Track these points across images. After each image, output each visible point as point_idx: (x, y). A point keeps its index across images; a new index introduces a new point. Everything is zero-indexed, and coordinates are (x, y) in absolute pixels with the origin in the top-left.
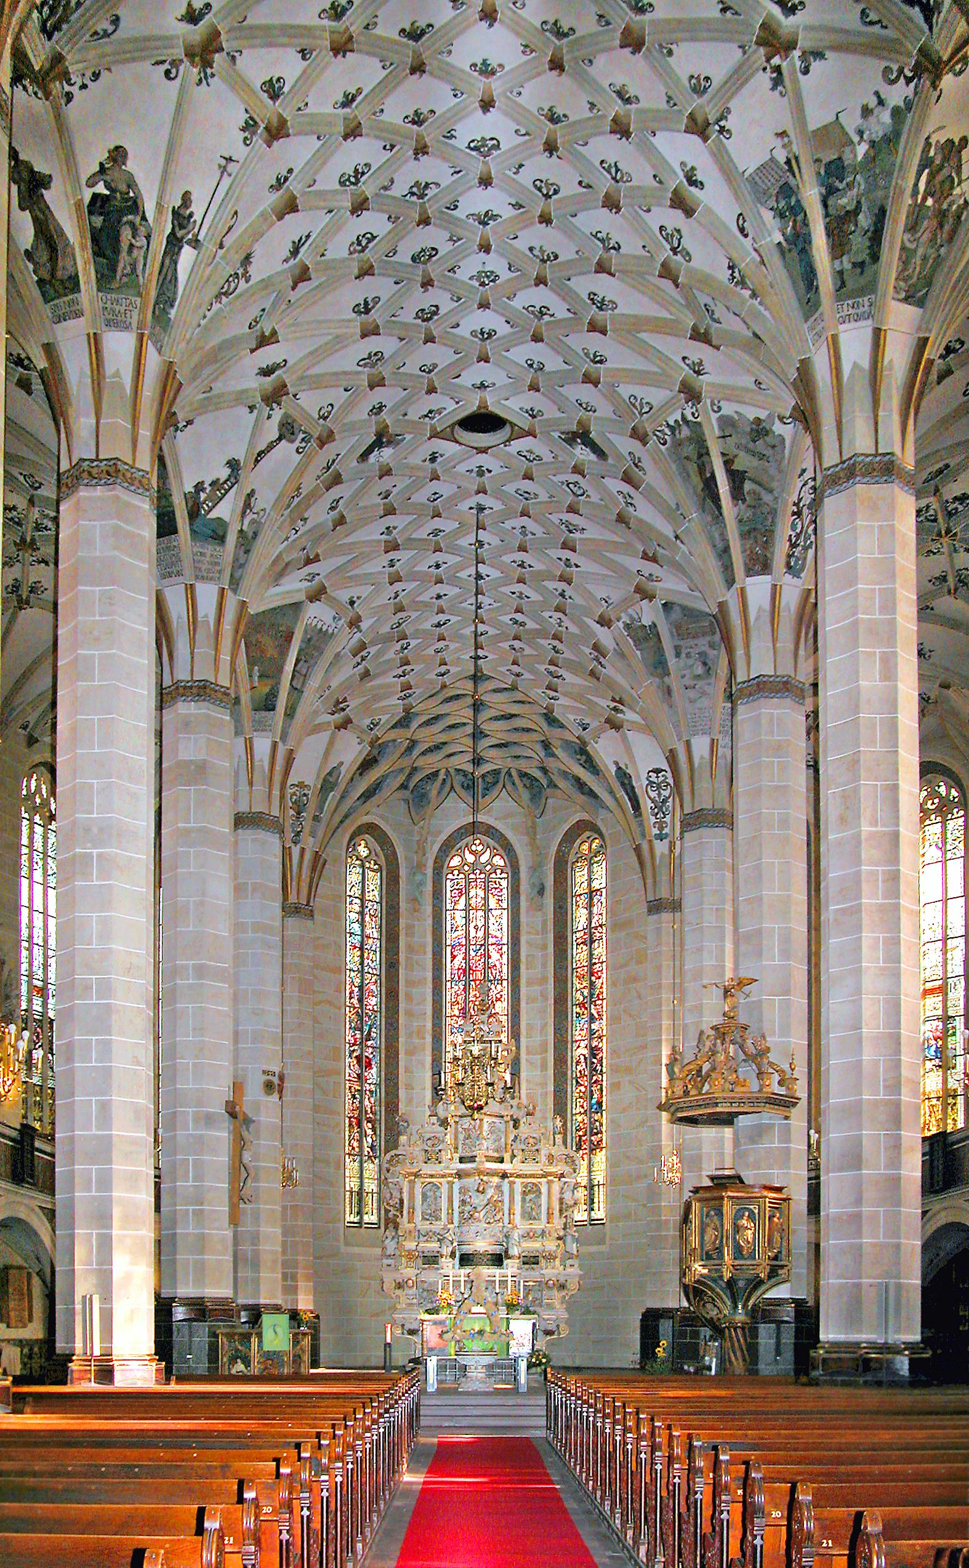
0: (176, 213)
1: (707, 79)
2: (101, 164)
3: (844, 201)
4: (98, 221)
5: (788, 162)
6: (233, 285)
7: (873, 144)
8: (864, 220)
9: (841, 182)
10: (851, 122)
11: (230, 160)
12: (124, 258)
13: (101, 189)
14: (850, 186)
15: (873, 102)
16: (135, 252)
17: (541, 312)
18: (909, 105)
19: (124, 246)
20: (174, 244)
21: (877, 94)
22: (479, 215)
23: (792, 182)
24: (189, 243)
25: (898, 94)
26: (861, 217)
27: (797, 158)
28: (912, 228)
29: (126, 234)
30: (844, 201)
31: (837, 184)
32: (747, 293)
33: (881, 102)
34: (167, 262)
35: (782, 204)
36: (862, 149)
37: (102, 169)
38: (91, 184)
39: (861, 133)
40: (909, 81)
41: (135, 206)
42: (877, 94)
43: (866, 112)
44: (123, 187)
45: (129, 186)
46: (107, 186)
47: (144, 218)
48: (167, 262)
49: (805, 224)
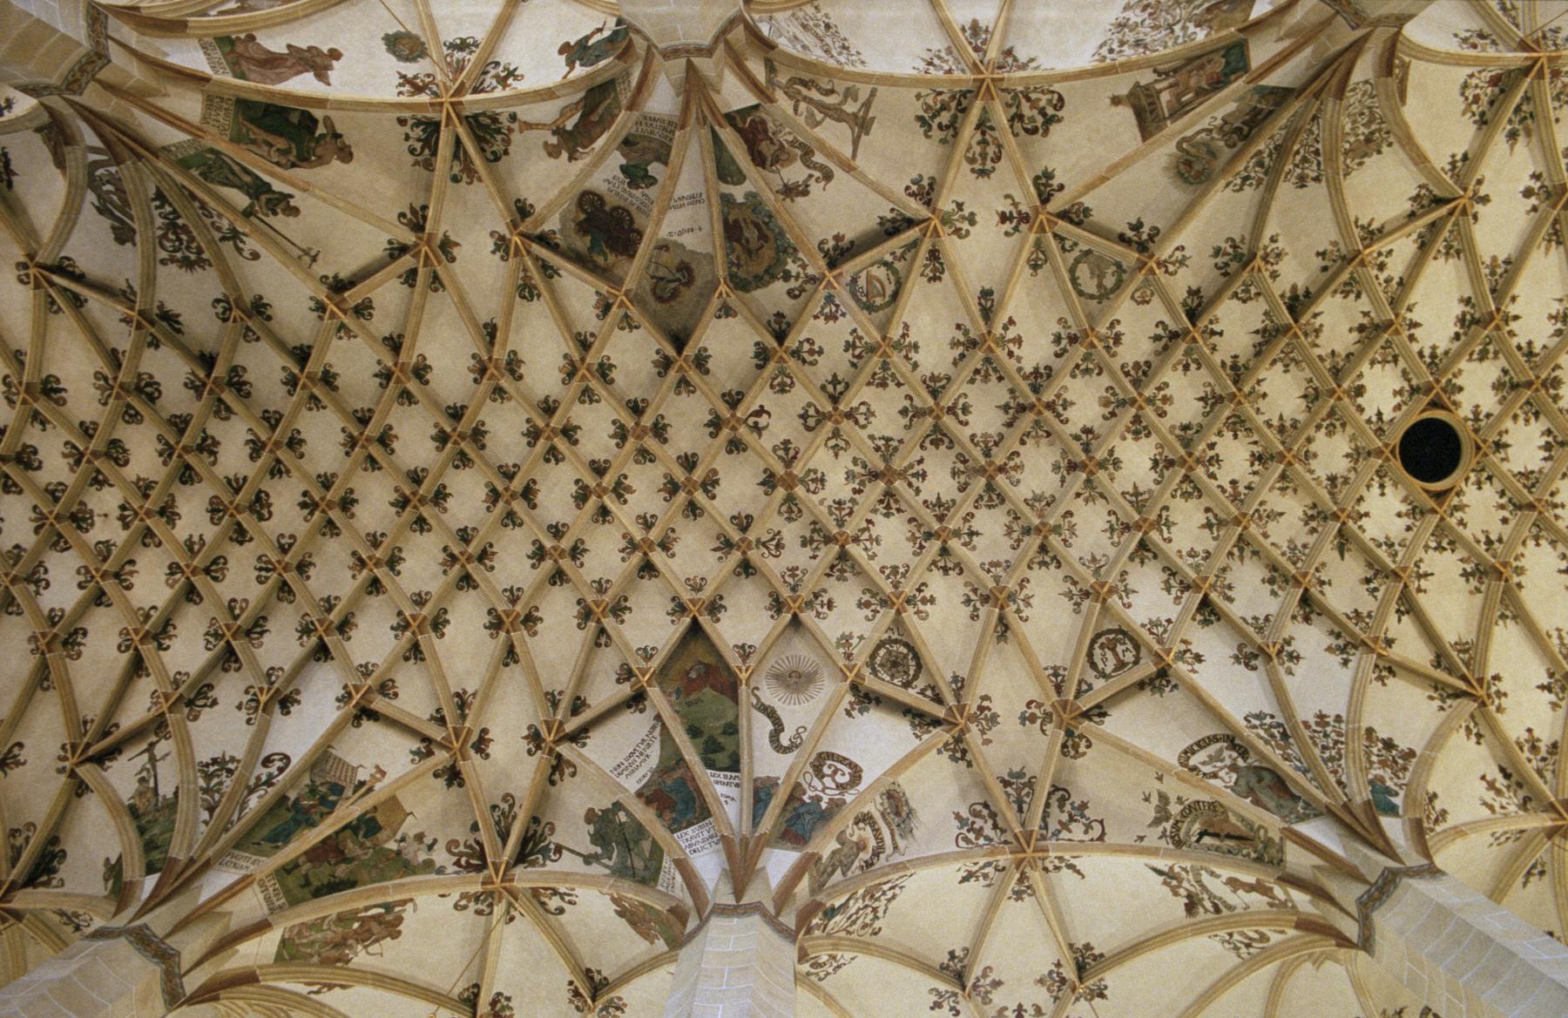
0: (286, 197)
1: (396, 695)
2: (340, 136)
3: (350, 845)
4: (294, 118)
5: (362, 784)
6: (168, 244)
7: (399, 853)
8: (342, 871)
9: (365, 836)
10: (409, 827)
11: (314, 259)
12: (262, 135)
13: (321, 130)
14: (362, 846)
15: (428, 840)
16: (266, 148)
17: (39, 581)
18: (441, 871)
19: (271, 138)
20: (258, 189)
21: (435, 841)
22: (173, 506)
23: (348, 792)
24: (251, 206)
25: (441, 857)
26: (343, 866)
27: (370, 790)
28: (342, 919)
29: (281, 143)
30: (350, 845)
31: (361, 833)
32: (202, 783)
33: (430, 847)
34: (247, 179)
35: (323, 789)
36: (392, 846)
37: (337, 136)
38: (327, 119)
39: (403, 840)
40: (457, 863)
41: (303, 159)
42: (435, 841)
43: (420, 837)
44: (319, 151)
45: (319, 157)
46: (322, 136)
47: (294, 165)
48: (247, 179)
49: (323, 816)
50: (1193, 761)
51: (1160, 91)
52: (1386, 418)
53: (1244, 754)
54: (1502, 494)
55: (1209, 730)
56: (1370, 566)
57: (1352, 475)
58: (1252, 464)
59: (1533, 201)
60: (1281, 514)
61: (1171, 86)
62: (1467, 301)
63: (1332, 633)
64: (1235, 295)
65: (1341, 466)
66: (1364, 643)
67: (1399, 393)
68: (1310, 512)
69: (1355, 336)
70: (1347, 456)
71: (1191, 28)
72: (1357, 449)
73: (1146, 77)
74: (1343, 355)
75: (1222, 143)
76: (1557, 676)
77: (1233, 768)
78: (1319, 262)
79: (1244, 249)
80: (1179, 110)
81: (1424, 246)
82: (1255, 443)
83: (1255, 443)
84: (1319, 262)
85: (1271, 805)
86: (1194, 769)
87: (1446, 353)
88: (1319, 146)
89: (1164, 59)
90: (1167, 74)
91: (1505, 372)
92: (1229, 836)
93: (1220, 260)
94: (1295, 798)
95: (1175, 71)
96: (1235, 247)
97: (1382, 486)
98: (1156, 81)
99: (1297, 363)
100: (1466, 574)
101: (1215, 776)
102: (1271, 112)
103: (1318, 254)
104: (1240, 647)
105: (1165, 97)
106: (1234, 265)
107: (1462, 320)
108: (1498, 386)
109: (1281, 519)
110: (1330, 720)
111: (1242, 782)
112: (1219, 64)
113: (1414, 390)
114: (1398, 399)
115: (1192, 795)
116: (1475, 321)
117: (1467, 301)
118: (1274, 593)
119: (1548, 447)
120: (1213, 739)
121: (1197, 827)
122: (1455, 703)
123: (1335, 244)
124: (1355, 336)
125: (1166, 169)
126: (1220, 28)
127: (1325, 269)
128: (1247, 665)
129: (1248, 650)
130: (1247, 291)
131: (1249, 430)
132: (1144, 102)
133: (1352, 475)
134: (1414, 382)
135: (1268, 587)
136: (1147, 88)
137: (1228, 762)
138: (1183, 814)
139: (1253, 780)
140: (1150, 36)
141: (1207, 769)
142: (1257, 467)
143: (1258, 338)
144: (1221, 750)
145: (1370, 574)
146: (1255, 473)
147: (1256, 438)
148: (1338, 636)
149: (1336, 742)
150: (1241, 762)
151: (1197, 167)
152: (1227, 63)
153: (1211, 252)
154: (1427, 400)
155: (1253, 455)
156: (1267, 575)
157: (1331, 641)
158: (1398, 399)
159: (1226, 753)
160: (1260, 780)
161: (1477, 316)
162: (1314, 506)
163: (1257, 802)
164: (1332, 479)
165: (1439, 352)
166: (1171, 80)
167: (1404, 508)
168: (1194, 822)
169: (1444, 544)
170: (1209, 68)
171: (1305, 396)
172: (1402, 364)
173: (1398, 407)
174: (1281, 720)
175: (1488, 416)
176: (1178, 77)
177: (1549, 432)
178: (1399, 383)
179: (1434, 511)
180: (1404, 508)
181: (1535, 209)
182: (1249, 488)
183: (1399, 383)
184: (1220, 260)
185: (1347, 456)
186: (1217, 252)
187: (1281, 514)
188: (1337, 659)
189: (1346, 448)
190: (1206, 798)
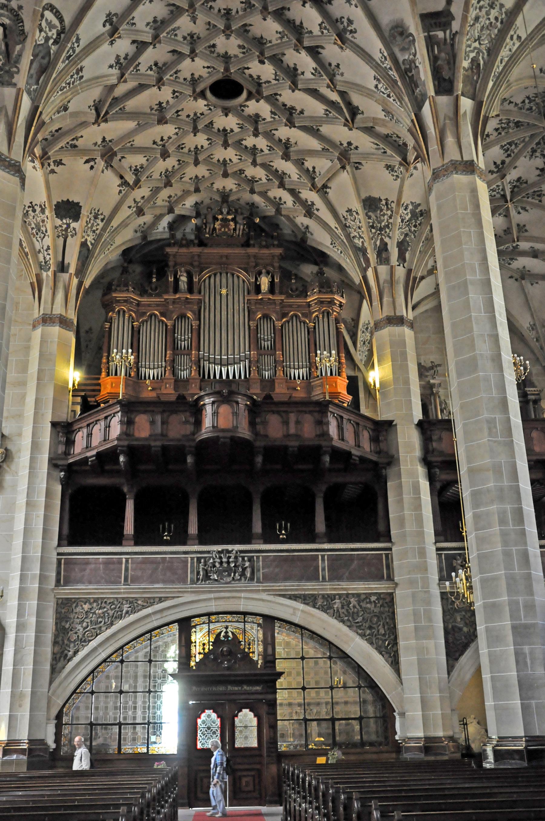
50: (48, 15)
51: (445, 33)
52: (246, 71)
53: (56, 42)
54: (202, 114)
55: (68, 20)
56: (165, 64)
57: (215, 55)
58: (224, 9)
59: (345, 145)
60: (195, 23)
61: (445, 39)
62: (302, 112)
63: (127, 55)
64: (323, 22)
65: (220, 49)
66: (122, 75)
67: (259, 77)
68: (195, 36)
69: (292, 66)
70: (226, 53)
71: (472, 55)
72: (230, 57)
73: (455, 26)
74: (283, 59)
75: (406, 57)
76: (110, 143)
77: (47, 39)
78: (334, 64)
79: (349, 36)
80: (430, 42)
81: (332, 104)
82: (237, 12)
83: (237, 12)
84: (334, 64)
85: (32, 71)
86: (42, 16)
87: (277, 100)
88: (391, 100)
89: (460, 42)
90: (453, 39)
91: (264, 119)
92: (7, 45)
93: (345, 21)
94: (37, 83)
95: (452, 45)
96: (351, 32)
97: (208, 67)
98: (451, 31)
99: (281, 38)
100: (160, 104)
101: (41, 30)
102: (414, 92)
103: (338, 65)
104: (116, 15)
105: (440, 34)
106: (341, 27)
107: (293, 108)
108: (257, 116)
109: (192, 23)
110: (81, 74)
111: (41, 48)
112: (446, 74)
113: (259, 85)
114: (255, 77)
115: (25, 15)
116: (291, 114)
117: (302, 112)
118: (148, 24)
119: (225, 130)
120: (61, 20)
121: (7, 21)
122: (93, 111)
123: (342, 74)
124: (292, 66)
125: (402, 20)
126: (466, 77)
127: (330, 65)
128: (106, 21)
129: (115, 19)
130: (325, 28)
131: (245, 10)
132: (443, 20)
133: (215, 55)
134: (264, 85)
135: (151, 19)
136: (450, 24)
137: (50, 34)
138: (12, 10)
139: (41, 55)
140: (478, 26)
141: (44, 24)
142: (223, 11)
143: (298, 23)
144: (54, 27)
145: (160, 65)
146: (219, 11)
147: (241, 13)
148: (125, 58)
149: (69, 84)
150: (51, 41)
151: (398, 38)
152: (445, 80)
153: (351, 18)
154: (254, 91)
155: (230, 10)
156: (159, 19)
157: (123, 56)
158: (255, 77)
159: (54, 31)
160: (43, 58)
161: (294, 115)
162: (199, 38)
163: (32, 62)
164: (214, 46)
165: (278, 97)
166: (448, 41)
167: (196, 76)
168: (10, 20)
169: (176, 94)
170: (446, 67)
171: (262, 37)
172: (274, 82)
173: (251, 76)
174: (78, 50)
175: (243, 110)
176: (449, 47)
177: (232, 131)
178: (263, 79)
179: (194, 91)
180: (196, 76)
181: (341, 144)
182: (211, 7)
183: (263, 79)
184: (345, 21)
185: (226, 53)
186: (350, 22)
187: (195, 23)
188: (113, 61)
189: (231, 52)
190: (27, 28)
